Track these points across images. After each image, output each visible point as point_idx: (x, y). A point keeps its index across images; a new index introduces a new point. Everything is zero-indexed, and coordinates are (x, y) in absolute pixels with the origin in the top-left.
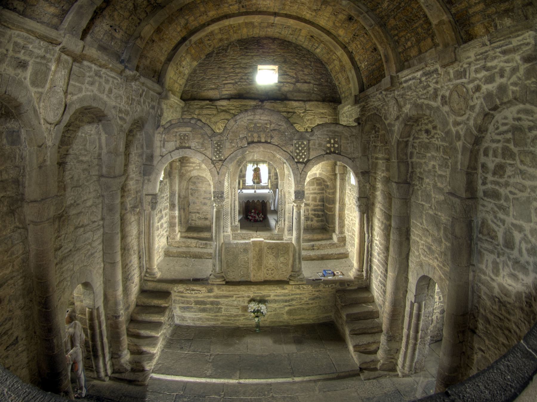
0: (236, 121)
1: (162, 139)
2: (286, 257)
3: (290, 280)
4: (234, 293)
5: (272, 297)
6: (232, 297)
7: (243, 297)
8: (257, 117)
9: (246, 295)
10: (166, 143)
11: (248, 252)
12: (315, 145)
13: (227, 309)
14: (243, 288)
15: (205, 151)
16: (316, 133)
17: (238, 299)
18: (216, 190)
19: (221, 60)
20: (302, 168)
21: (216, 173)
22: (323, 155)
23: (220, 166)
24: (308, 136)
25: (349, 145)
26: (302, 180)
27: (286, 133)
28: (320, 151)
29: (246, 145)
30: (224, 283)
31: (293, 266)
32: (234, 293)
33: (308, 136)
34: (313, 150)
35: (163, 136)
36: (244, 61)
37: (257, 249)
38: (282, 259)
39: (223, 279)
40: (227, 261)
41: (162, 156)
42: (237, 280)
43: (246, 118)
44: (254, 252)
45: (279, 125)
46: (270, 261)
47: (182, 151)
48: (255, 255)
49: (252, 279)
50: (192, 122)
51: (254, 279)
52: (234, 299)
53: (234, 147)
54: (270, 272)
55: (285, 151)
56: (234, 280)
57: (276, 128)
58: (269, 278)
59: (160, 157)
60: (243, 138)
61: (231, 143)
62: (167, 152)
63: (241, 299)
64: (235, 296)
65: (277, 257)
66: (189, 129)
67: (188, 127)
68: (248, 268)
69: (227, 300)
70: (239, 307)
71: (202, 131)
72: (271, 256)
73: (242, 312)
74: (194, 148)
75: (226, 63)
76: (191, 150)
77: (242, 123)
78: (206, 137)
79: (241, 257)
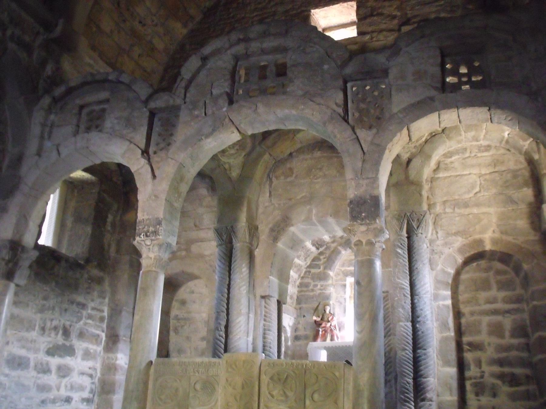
0: (205, 59)
1: (49, 123)
8: (255, 46)
11: (214, 390)
21: (150, 175)
22: (432, 99)
26: (368, 166)
36: (281, 9)
37: (239, 381)
43: (229, 52)
44: (230, 389)
50: (110, 78)
53: (197, 116)
60: (220, 95)
66: (103, 95)
77: (220, 63)
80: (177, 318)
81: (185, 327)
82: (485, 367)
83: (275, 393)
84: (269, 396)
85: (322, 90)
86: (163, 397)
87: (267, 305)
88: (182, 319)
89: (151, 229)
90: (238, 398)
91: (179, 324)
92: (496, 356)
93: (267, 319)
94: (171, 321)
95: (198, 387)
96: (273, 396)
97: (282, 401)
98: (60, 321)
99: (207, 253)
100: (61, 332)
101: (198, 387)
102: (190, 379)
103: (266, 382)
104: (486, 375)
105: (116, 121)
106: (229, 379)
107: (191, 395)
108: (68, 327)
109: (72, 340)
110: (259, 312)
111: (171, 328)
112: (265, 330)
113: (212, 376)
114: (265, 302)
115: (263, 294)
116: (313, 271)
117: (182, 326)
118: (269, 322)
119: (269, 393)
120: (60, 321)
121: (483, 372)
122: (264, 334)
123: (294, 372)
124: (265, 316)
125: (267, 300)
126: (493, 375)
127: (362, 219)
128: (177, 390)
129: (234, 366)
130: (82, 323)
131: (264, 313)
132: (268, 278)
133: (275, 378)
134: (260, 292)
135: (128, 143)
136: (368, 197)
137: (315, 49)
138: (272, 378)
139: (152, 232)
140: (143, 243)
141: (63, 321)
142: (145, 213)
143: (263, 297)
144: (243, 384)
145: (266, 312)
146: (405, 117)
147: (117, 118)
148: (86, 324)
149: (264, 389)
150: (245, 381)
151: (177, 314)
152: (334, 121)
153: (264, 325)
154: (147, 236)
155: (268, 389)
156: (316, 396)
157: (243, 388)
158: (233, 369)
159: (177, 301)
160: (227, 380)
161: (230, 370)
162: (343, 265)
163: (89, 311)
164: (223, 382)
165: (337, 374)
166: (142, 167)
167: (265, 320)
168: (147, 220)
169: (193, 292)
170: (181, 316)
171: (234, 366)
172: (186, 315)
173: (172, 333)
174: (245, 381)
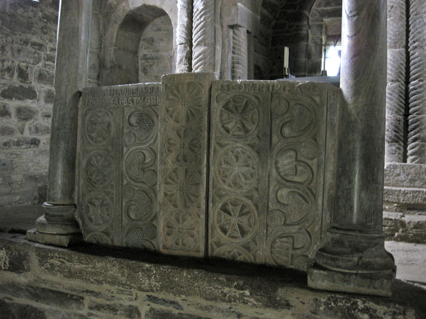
2: (305, 151)
3: (317, 266)
6: (79, 300)
30: (65, 241)
31: (339, 200)
37: (182, 110)
38: (286, 162)
39: (70, 230)
40: (89, 163)
42: (117, 243)
44: (171, 122)
46: (234, 166)
48: (173, 135)
49: (163, 242)
51: (170, 241)
54: (234, 220)
56: (107, 240)
58: (228, 246)
64: (88, 300)
65: (263, 148)
68: (150, 194)
72: (240, 146)
79: (131, 149)
80: (145, 57)
81: (154, 66)
83: (230, 126)
84: (222, 130)
86: (94, 135)
87: (235, 36)
88: (150, 58)
90: (182, 133)
91: (148, 64)
93: (236, 51)
94: (139, 61)
95: (133, 120)
96: (228, 131)
97: (239, 137)
98: (13, 62)
100: (16, 74)
101: (133, 120)
102: (123, 111)
103: (219, 113)
106: (171, 109)
107: (125, 131)
108: (25, 69)
109: (31, 83)
110: (227, 43)
111: (140, 69)
112: (233, 63)
113: (150, 106)
114: (234, 33)
115: (231, 23)
116: (290, 11)
117: (151, 66)
118: (238, 54)
119: (223, 127)
120: (13, 62)
122: (233, 67)
123: (257, 98)
124: (234, 48)
125: (236, 31)
128: (109, 125)
129: (175, 92)
130: (40, 64)
131: (232, 45)
132: (236, 5)
133: (231, 106)
134: (228, 21)
138: (226, 107)
141: (16, 63)
143: (232, 27)
144: (188, 115)
145: (234, 44)
148: (45, 66)
149: (216, 119)
150: (191, 111)
151: (145, 53)
153: (233, 58)
155: (221, 121)
156: (287, 131)
157: (188, 120)
158: (175, 95)
159: (144, 40)
160: (168, 111)
161: (171, 97)
162: (319, 6)
163: (48, 52)
164: (162, 113)
165: (317, 99)
167: (233, 53)
170: (149, 55)
171: (175, 92)
172: (154, 54)
174: (191, 111)
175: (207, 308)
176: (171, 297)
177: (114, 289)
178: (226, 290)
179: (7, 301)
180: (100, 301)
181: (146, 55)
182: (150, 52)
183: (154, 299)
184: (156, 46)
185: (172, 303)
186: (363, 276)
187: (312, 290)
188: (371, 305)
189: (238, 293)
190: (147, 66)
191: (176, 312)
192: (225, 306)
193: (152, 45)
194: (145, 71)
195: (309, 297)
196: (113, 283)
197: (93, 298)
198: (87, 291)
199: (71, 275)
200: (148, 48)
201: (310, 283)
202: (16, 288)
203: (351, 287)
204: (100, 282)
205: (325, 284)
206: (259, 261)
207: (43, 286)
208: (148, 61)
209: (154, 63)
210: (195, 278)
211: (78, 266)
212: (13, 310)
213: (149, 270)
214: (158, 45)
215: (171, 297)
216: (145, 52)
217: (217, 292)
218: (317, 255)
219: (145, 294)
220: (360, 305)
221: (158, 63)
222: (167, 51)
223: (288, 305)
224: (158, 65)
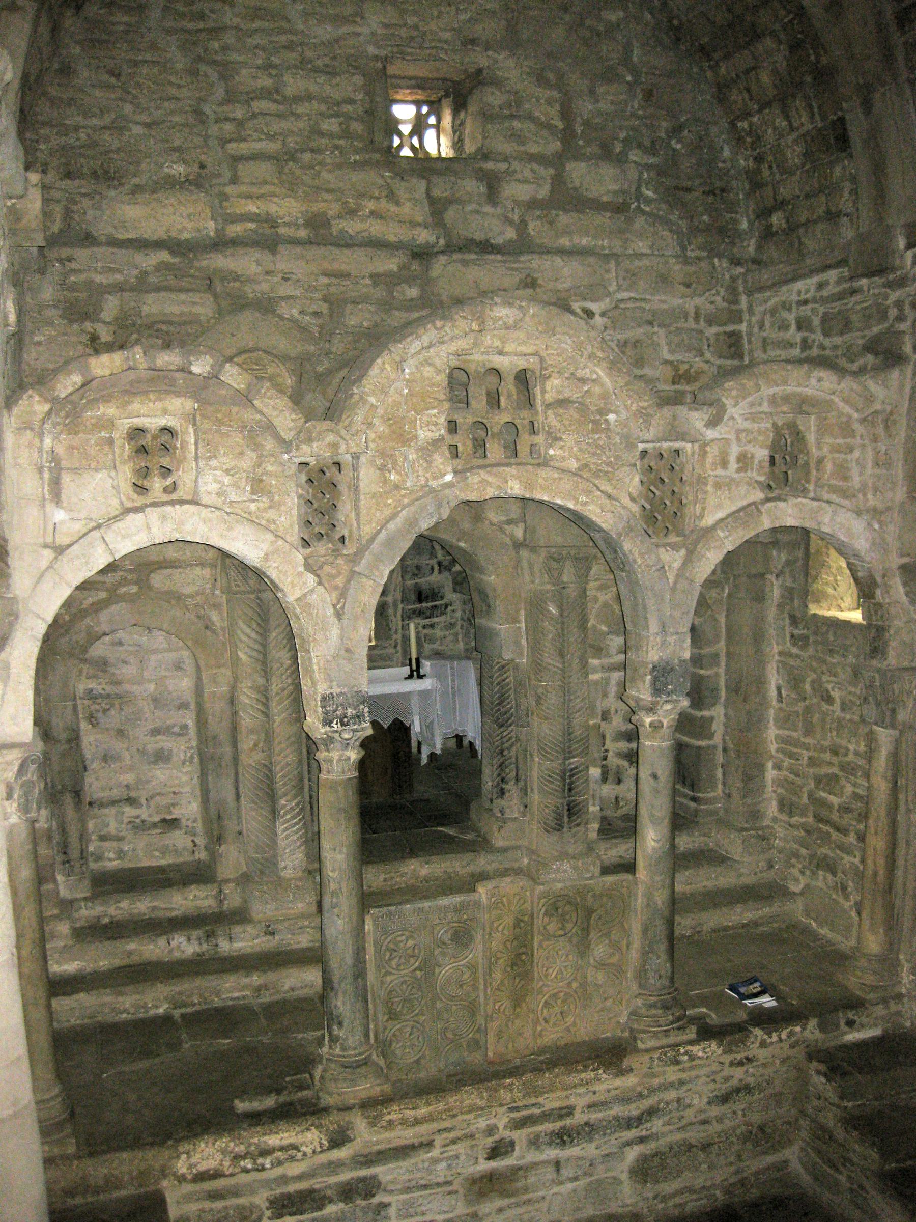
4: (435, 1126)
5: (578, 1110)
6: (430, 1144)
7: (472, 1136)
9: (482, 1123)
10: (66, 478)
12: (724, 464)
13: (410, 1204)
14: (470, 1097)
15: (271, 514)
16: (731, 411)
17: (453, 1150)
18: (336, 690)
19: (202, 16)
20: (676, 565)
23: (340, 581)
24: (699, 425)
25: (857, 454)
27: (612, 417)
28: (743, 489)
29: (449, 478)
32: (435, 1126)
33: (699, 425)
34: (718, 486)
35: (48, 442)
41: (60, 550)
45: (583, 380)
47: (164, 518)
51: (501, 1049)
52: (435, 1153)
55: (610, 497)
57: (567, 394)
59: (48, 554)
61: (382, 469)
62: (79, 527)
63: (460, 1148)
64: (439, 1140)
67: (178, 394)
69: (405, 1164)
70: (455, 1186)
71: (248, 415)
73: (469, 1202)
74: (219, 502)
75: (229, 38)
76: (205, 512)
78: (269, 444)
81: (113, 712)
82: (609, 744)
85: (609, 464)
88: (101, 696)
89: (350, 712)
91: (97, 707)
92: (623, 728)
99: (187, 590)
104: (610, 754)
105: (227, 480)
117: (105, 711)
121: (607, 751)
126: (619, 755)
127: (669, 694)
135: (270, 537)
136: (676, 661)
137: (595, 376)
139: (354, 717)
140: (336, 736)
142: (335, 683)
146: (726, 537)
147: (227, 472)
152: (632, 534)
154: (343, 724)
166: (312, 591)
168: (339, 695)
169: (120, 643)
172: (109, 689)
173: (84, 725)
175: (567, 1097)
176: (533, 1100)
177: (470, 1116)
178: (583, 1075)
179: (317, 1186)
180: (452, 1135)
181: (91, 690)
182: (100, 684)
183: (512, 1110)
184: (113, 674)
185: (533, 1105)
186: (679, 1028)
187: (647, 1051)
188: (689, 1048)
189: (592, 1074)
190: (98, 711)
191: (536, 1111)
192: (582, 1090)
193: (105, 671)
194: (92, 719)
195: (646, 1057)
196: (470, 1112)
197: (445, 1135)
198: (439, 1131)
199: (417, 1122)
200: (95, 677)
201: (640, 1045)
202: (334, 1167)
203: (671, 1040)
204: (454, 1116)
205: (651, 1043)
206: (579, 1040)
207: (376, 1148)
208: (99, 701)
209: (112, 705)
210: (557, 1076)
211: (423, 1111)
212: (329, 1193)
213: (511, 1085)
214: (117, 672)
215: (533, 1100)
216: (92, 685)
217: (576, 1081)
218: (629, 1019)
219: (504, 1109)
220: (682, 1051)
221: (120, 704)
222: (140, 683)
223: (631, 1070)
224: (121, 709)
